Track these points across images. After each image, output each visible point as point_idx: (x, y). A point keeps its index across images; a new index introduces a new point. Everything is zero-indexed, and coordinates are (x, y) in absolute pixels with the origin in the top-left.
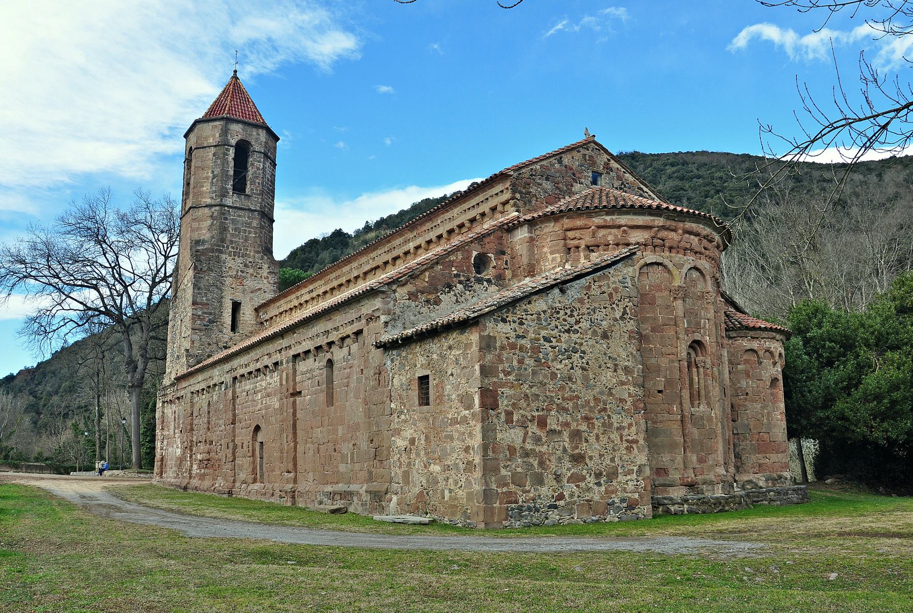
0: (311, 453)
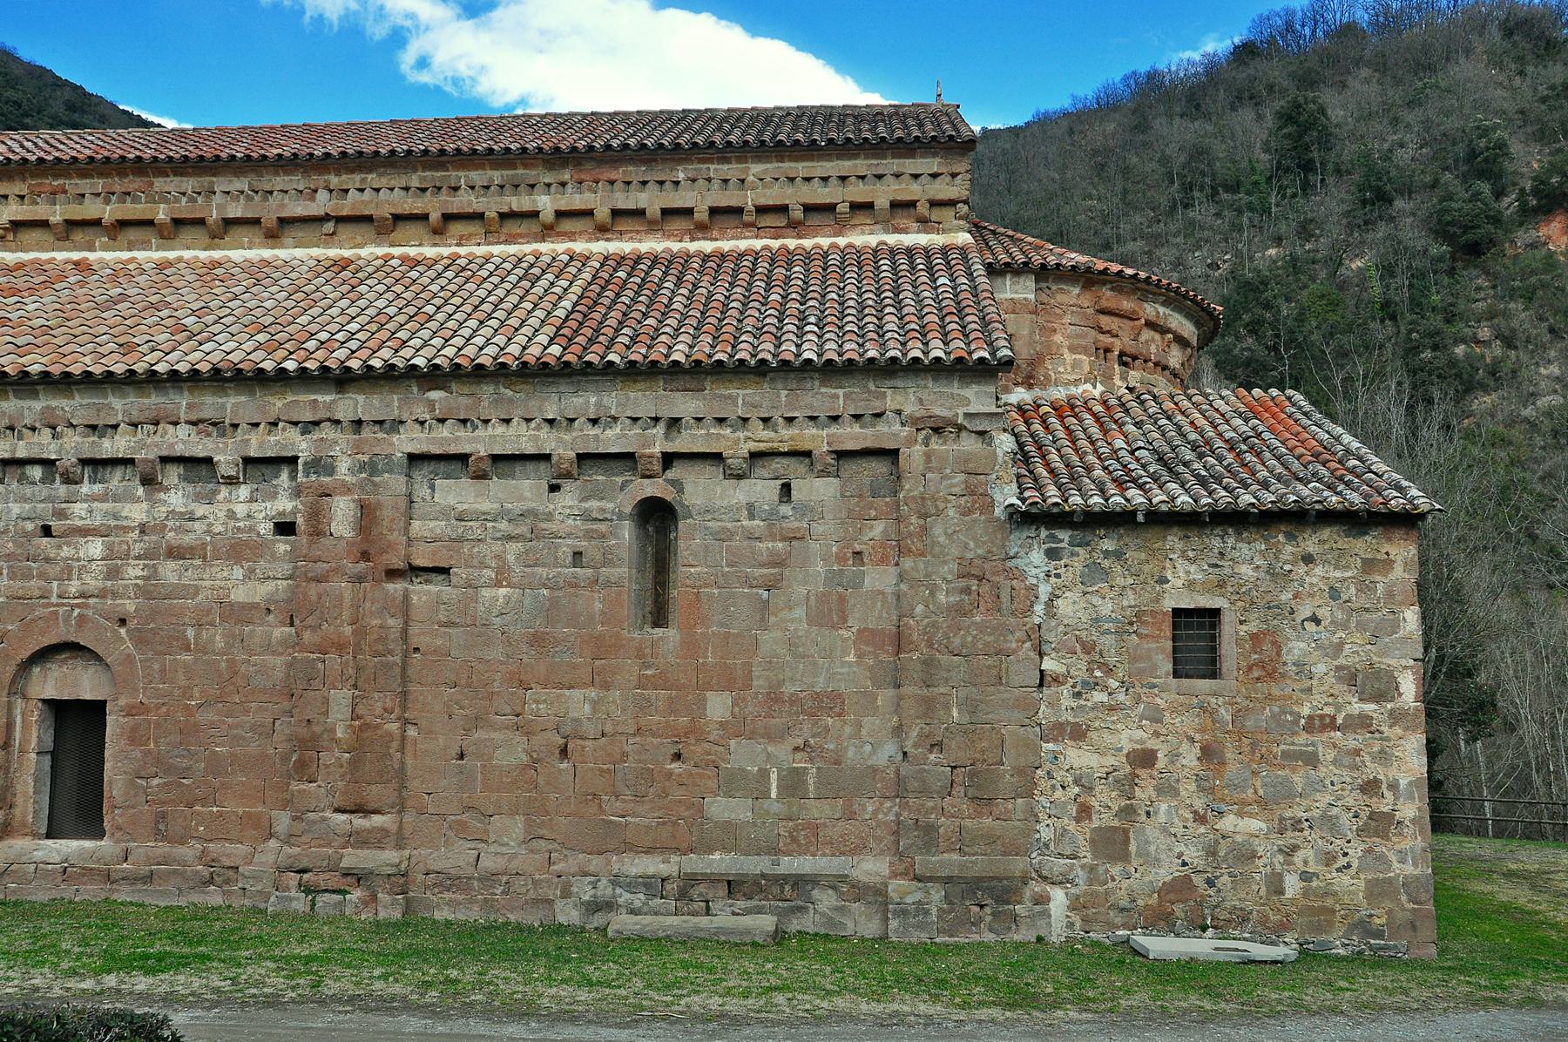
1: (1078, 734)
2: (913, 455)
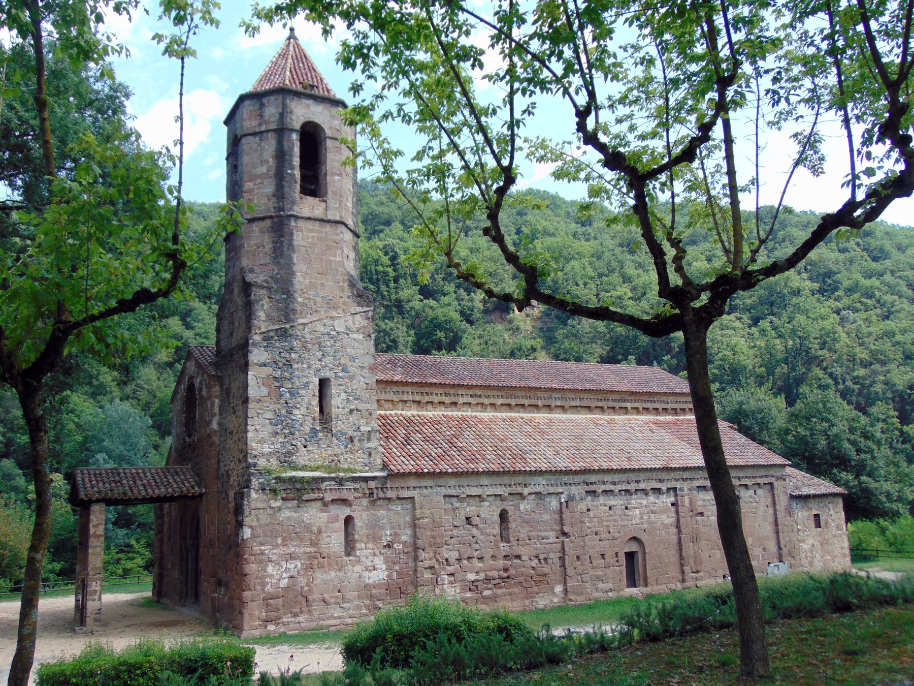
1: (804, 541)
2: (776, 484)
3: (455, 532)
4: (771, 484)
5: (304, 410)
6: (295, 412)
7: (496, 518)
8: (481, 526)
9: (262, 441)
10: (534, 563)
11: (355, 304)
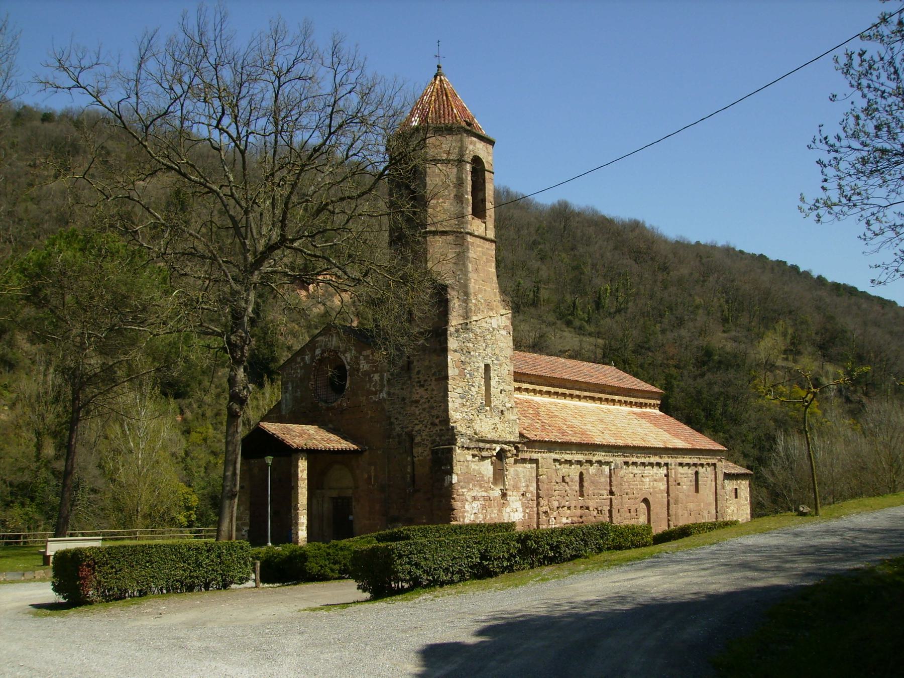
0: (686, 515)
2: (718, 464)
3: (557, 487)
4: (714, 465)
5: (477, 389)
6: (473, 389)
7: (577, 478)
8: (570, 483)
9: (456, 410)
10: (595, 513)
11: (502, 307)
